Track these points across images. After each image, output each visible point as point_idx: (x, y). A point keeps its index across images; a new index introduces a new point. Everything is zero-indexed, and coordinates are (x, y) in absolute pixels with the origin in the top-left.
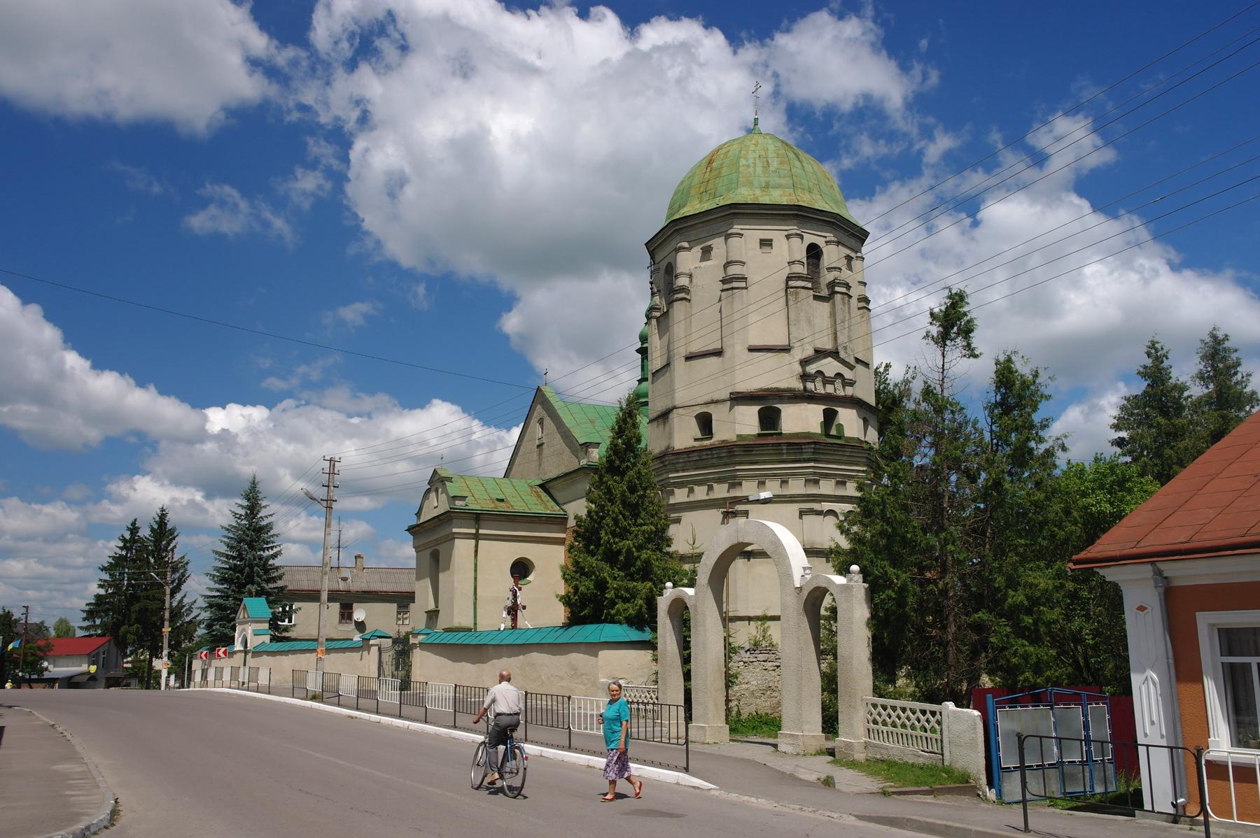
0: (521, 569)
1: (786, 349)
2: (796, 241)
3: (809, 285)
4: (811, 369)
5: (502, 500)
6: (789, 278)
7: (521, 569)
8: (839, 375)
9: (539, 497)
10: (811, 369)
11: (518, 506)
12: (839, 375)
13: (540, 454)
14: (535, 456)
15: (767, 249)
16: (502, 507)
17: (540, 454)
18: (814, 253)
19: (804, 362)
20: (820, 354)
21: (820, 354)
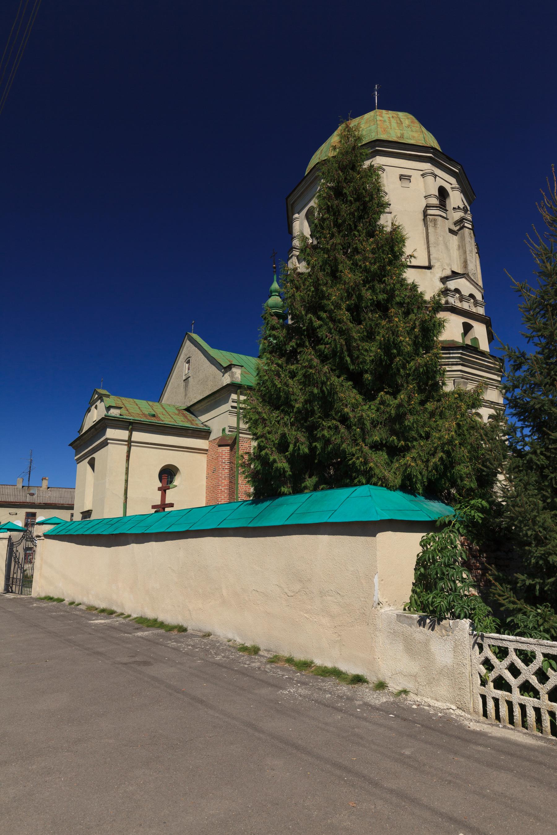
0: (168, 474)
1: (429, 268)
2: (430, 179)
3: (444, 215)
4: (452, 285)
5: (154, 416)
6: (428, 207)
7: (168, 474)
8: (472, 296)
9: (186, 417)
10: (452, 285)
11: (167, 420)
12: (472, 296)
13: (186, 386)
14: (182, 389)
15: (405, 183)
16: (154, 420)
17: (186, 386)
18: (443, 193)
19: (444, 280)
20: (455, 275)
21: (455, 275)
